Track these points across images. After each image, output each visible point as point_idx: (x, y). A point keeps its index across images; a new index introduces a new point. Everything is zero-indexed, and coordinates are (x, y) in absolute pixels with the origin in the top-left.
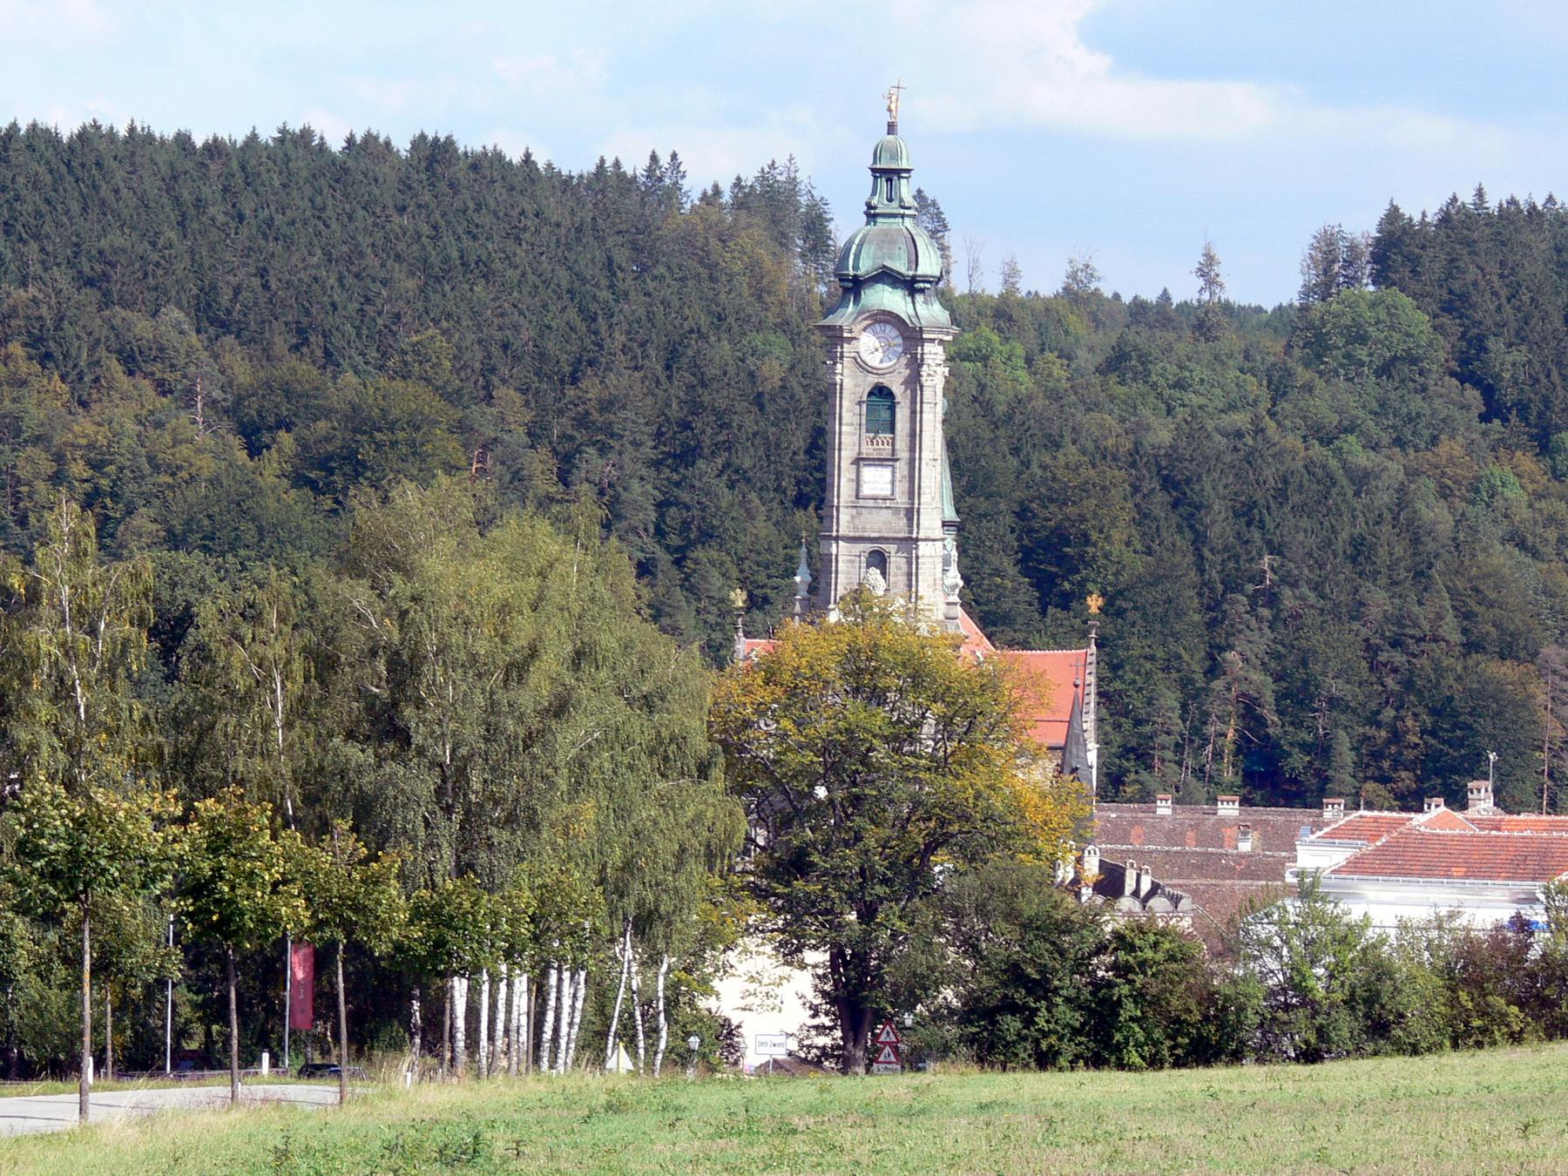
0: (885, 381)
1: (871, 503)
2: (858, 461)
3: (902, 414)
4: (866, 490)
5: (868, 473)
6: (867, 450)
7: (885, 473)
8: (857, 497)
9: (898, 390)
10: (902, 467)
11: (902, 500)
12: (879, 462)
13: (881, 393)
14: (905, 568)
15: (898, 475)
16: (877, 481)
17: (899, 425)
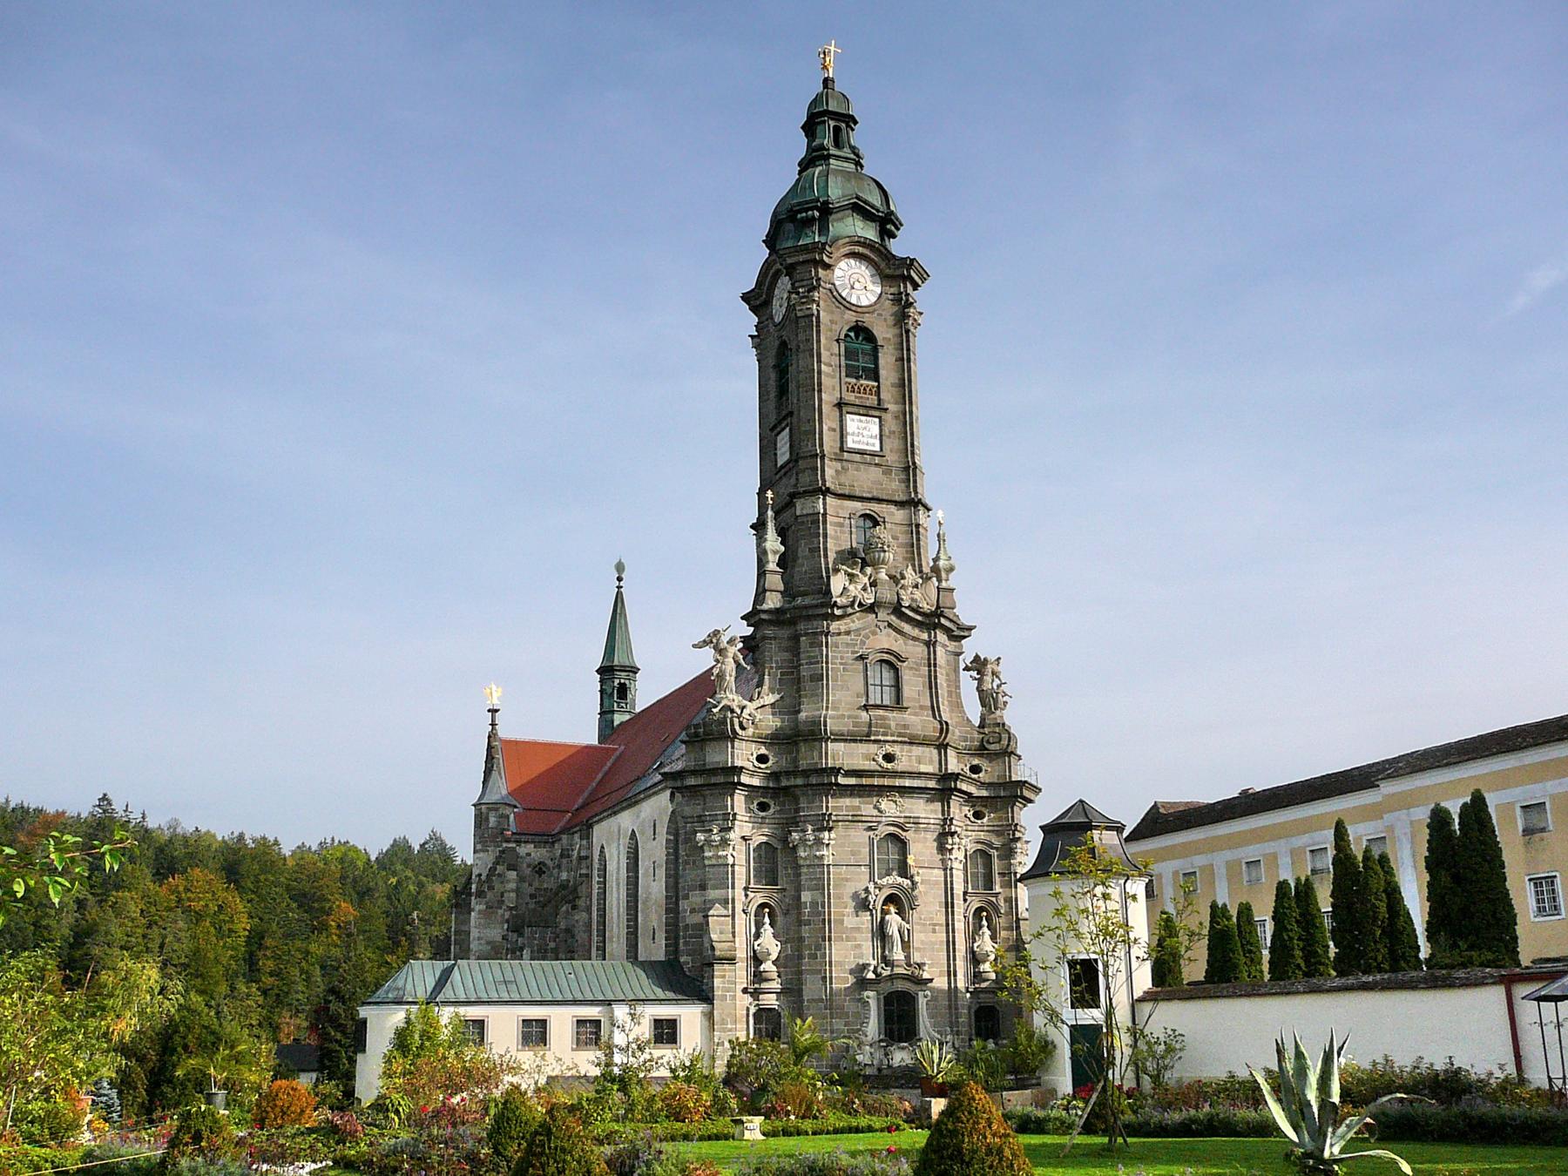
0: (867, 320)
1: (857, 457)
2: (840, 405)
3: (887, 360)
4: (851, 443)
5: (853, 423)
6: (850, 397)
7: (873, 426)
8: (842, 449)
9: (883, 331)
10: (892, 424)
11: (892, 458)
12: (865, 411)
13: (861, 332)
14: (903, 539)
15: (886, 431)
16: (863, 432)
17: (882, 373)
